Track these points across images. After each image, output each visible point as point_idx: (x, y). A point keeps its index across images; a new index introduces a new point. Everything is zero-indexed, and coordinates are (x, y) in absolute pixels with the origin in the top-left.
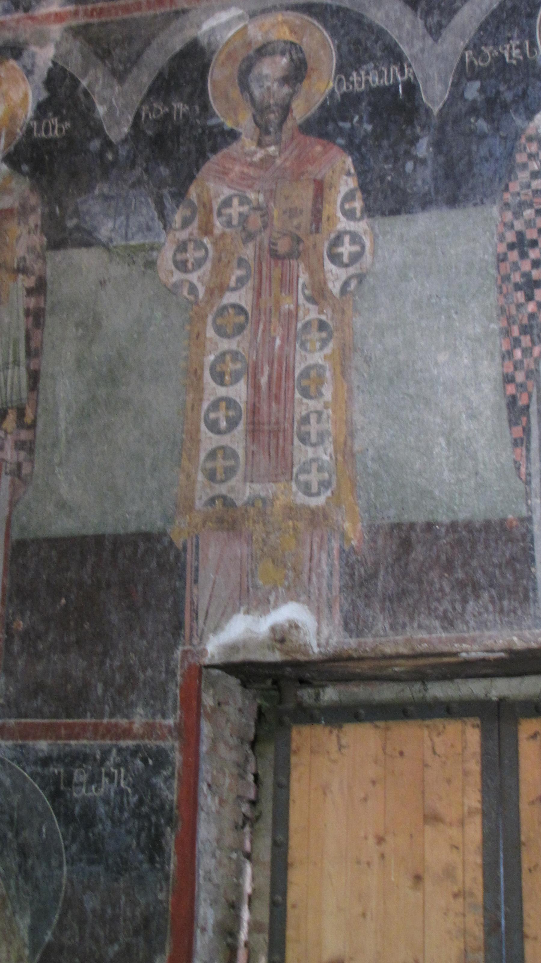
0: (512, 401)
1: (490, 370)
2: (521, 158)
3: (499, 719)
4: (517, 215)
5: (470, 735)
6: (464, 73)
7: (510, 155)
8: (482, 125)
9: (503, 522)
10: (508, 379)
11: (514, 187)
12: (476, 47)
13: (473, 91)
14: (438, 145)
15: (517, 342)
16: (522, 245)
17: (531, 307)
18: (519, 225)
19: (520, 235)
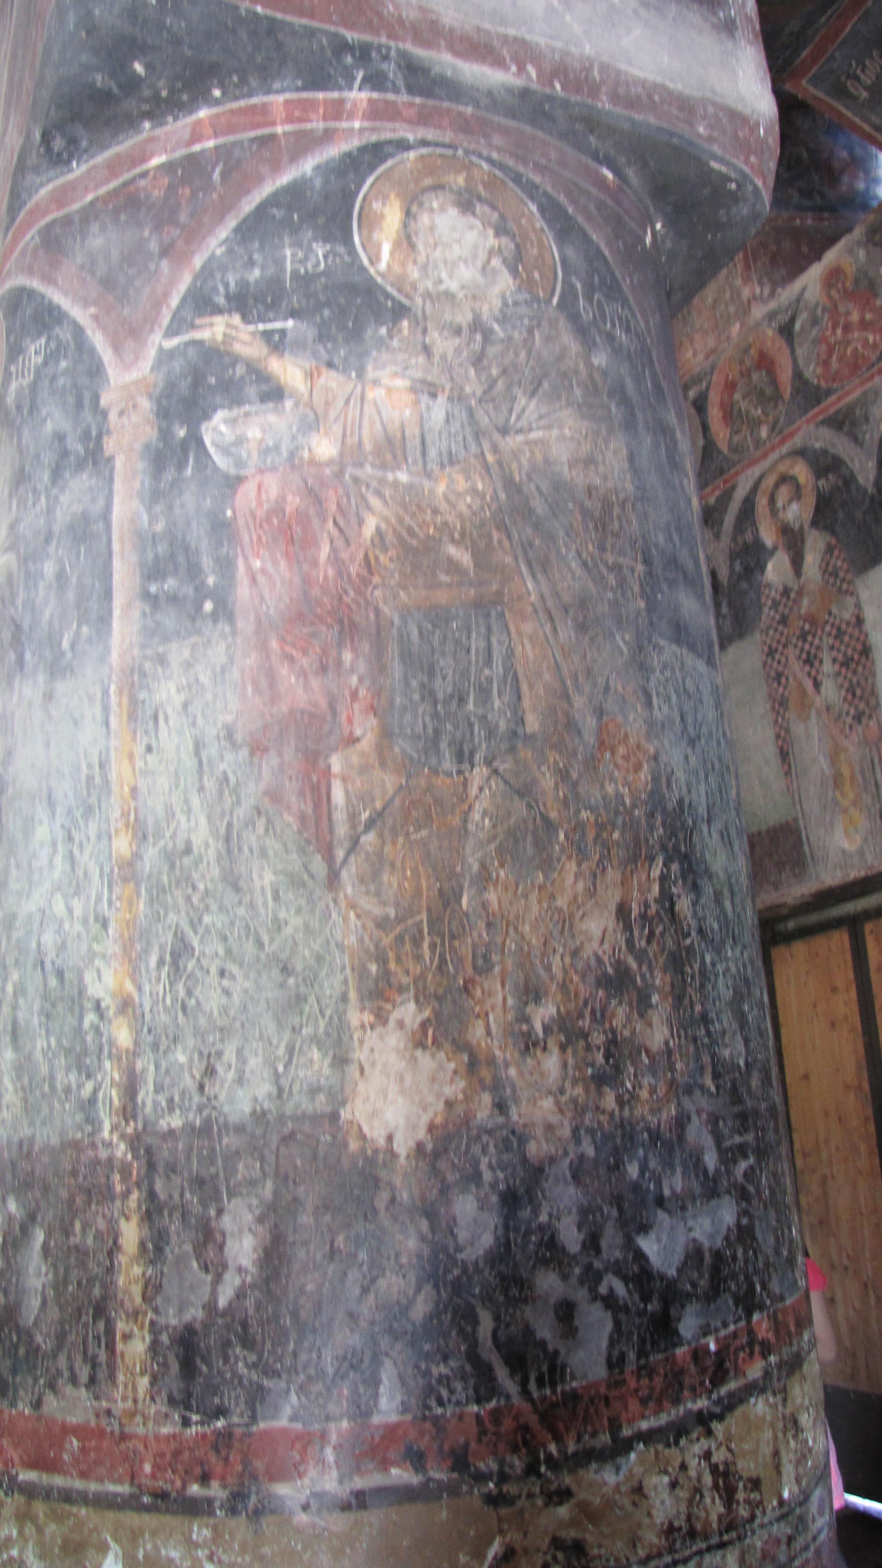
0: (781, 749)
1: (770, 733)
2: (763, 599)
3: (854, 925)
4: (767, 635)
5: (840, 939)
6: (733, 556)
7: (759, 600)
8: (744, 585)
9: (787, 823)
10: (778, 736)
11: (764, 618)
12: (734, 539)
13: (738, 567)
14: (729, 604)
15: (778, 713)
16: (771, 653)
17: (781, 690)
18: (768, 641)
19: (770, 647)
